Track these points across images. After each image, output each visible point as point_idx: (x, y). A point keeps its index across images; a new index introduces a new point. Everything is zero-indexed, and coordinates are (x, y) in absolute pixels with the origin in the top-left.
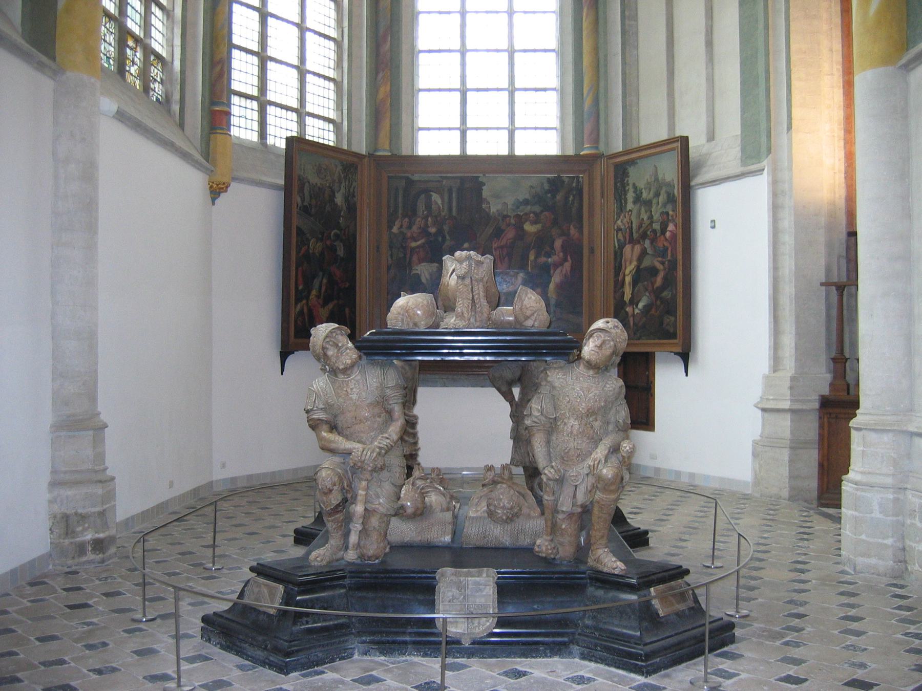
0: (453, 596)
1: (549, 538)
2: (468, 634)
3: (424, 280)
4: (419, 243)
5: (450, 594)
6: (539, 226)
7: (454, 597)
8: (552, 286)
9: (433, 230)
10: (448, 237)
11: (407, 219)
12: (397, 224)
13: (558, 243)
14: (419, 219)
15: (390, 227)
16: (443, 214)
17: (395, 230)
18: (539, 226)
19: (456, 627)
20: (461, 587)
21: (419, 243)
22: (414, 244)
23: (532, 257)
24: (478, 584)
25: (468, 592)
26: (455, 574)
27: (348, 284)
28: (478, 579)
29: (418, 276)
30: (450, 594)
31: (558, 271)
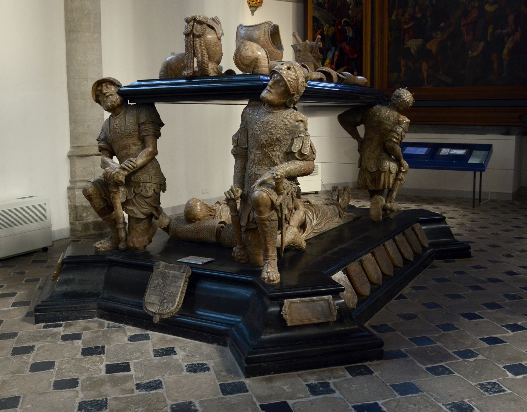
0: (158, 283)
1: (241, 246)
2: (159, 314)
3: (412, 51)
4: (409, 25)
5: (156, 282)
6: (496, 6)
7: (158, 285)
8: (505, 51)
9: (419, 15)
10: (429, 20)
11: (401, 10)
12: (395, 13)
13: (511, 18)
14: (409, 9)
15: (390, 16)
16: (426, 3)
17: (393, 17)
18: (496, 6)
19: (152, 308)
20: (164, 276)
21: (409, 25)
22: (406, 27)
23: (490, 30)
24: (175, 277)
25: (168, 282)
26: (166, 267)
27: (356, 56)
28: (176, 273)
29: (409, 49)
30: (156, 282)
31: (511, 39)
